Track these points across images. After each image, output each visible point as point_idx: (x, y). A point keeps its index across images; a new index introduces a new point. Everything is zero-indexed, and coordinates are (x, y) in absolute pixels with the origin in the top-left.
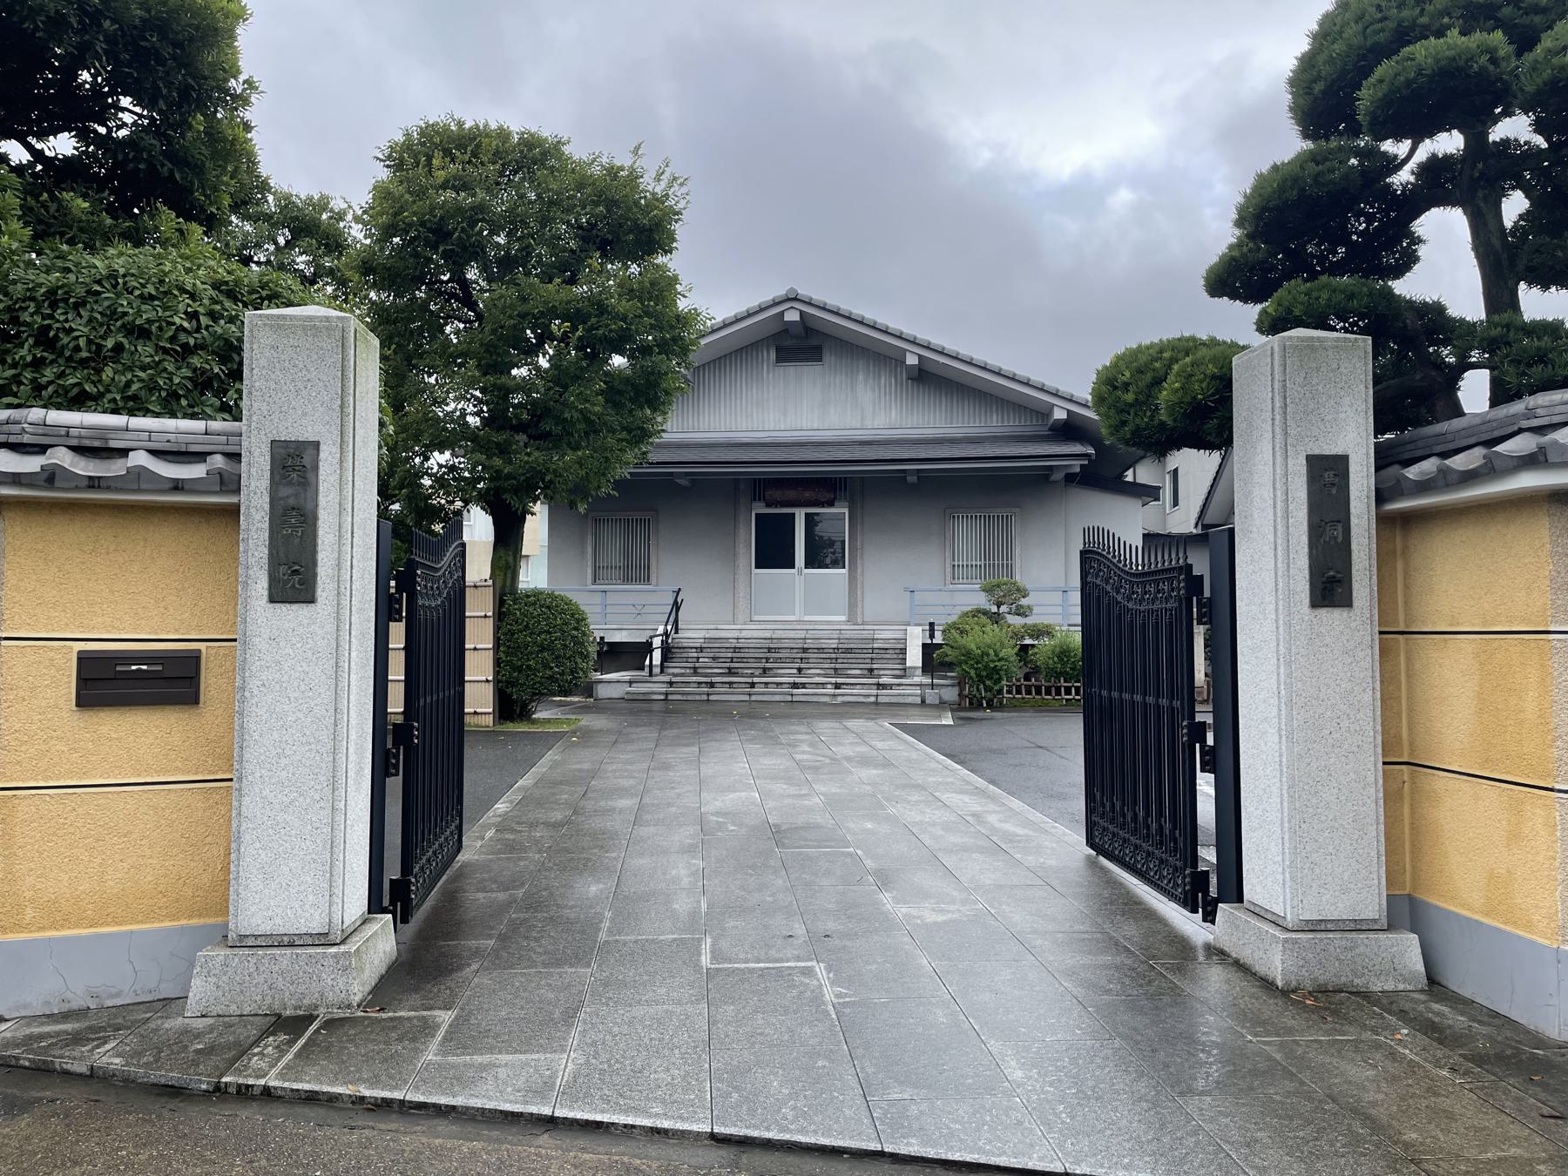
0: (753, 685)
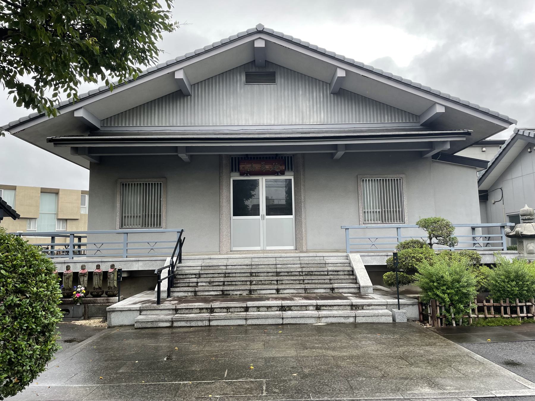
0: (247, 309)
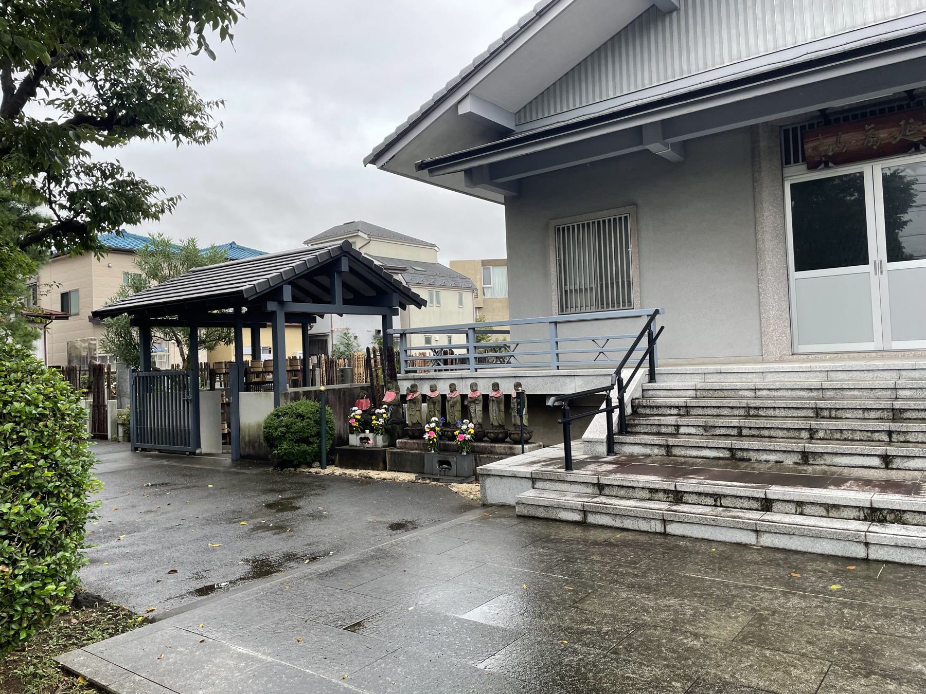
0: (767, 505)
